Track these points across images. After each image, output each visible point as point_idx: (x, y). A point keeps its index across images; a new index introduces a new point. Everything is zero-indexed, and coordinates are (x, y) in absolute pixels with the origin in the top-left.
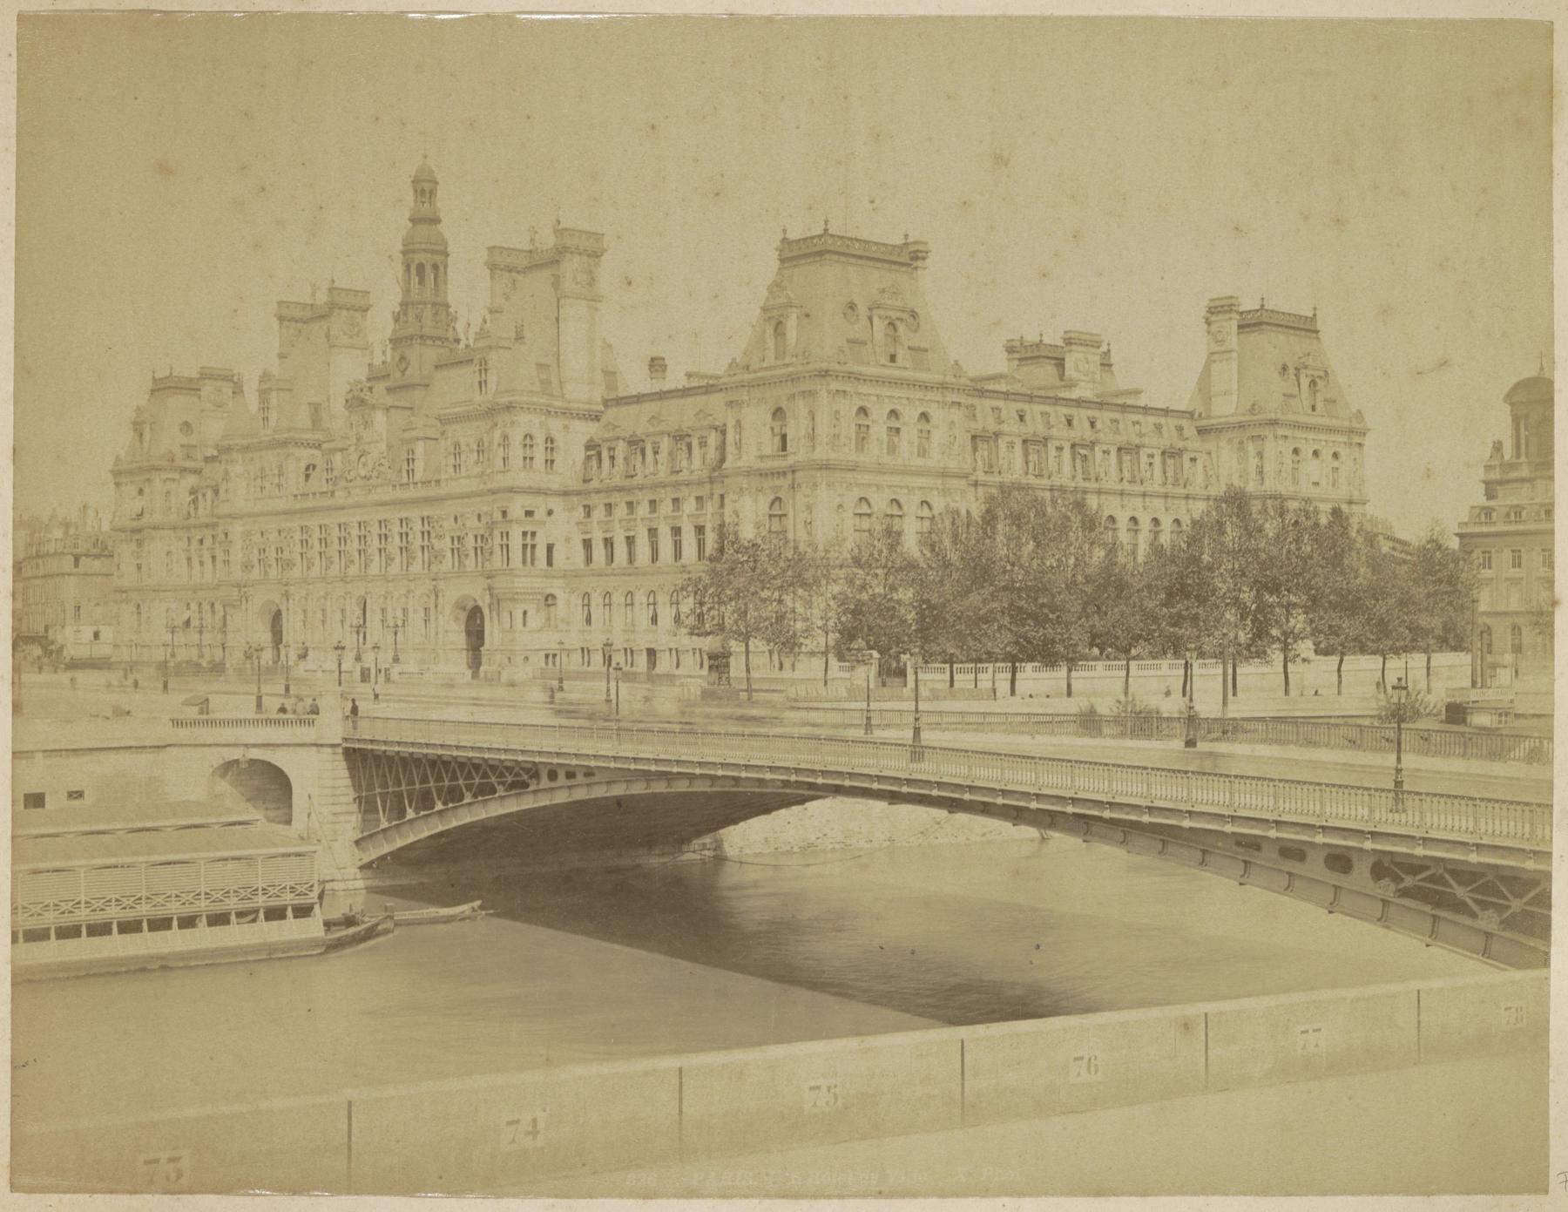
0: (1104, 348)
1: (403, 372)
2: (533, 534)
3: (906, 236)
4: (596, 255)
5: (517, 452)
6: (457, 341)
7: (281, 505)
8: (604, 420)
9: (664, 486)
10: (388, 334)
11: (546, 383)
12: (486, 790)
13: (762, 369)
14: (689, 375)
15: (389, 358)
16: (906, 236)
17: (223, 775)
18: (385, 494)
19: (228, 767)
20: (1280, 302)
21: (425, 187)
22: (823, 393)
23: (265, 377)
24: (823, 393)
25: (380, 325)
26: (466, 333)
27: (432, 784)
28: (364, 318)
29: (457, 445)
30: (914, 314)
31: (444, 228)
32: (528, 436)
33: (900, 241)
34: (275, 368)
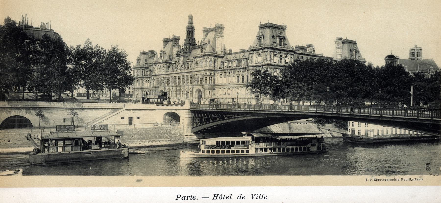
0: (313, 47)
1: (186, 50)
2: (211, 78)
3: (283, 24)
5: (208, 63)
6: (196, 45)
7: (164, 73)
8: (224, 58)
9: (236, 69)
10: (184, 43)
11: (214, 51)
12: (222, 118)
13: (256, 47)
14: (241, 50)
15: (184, 48)
16: (283, 24)
17: (167, 115)
18: (183, 71)
20: (350, 38)
21: (191, 18)
22: (269, 51)
23: (161, 51)
24: (269, 51)
25: (182, 42)
26: (198, 43)
27: (210, 117)
28: (179, 41)
29: (197, 62)
30: (284, 38)
31: (194, 25)
32: (211, 60)
34: (163, 49)
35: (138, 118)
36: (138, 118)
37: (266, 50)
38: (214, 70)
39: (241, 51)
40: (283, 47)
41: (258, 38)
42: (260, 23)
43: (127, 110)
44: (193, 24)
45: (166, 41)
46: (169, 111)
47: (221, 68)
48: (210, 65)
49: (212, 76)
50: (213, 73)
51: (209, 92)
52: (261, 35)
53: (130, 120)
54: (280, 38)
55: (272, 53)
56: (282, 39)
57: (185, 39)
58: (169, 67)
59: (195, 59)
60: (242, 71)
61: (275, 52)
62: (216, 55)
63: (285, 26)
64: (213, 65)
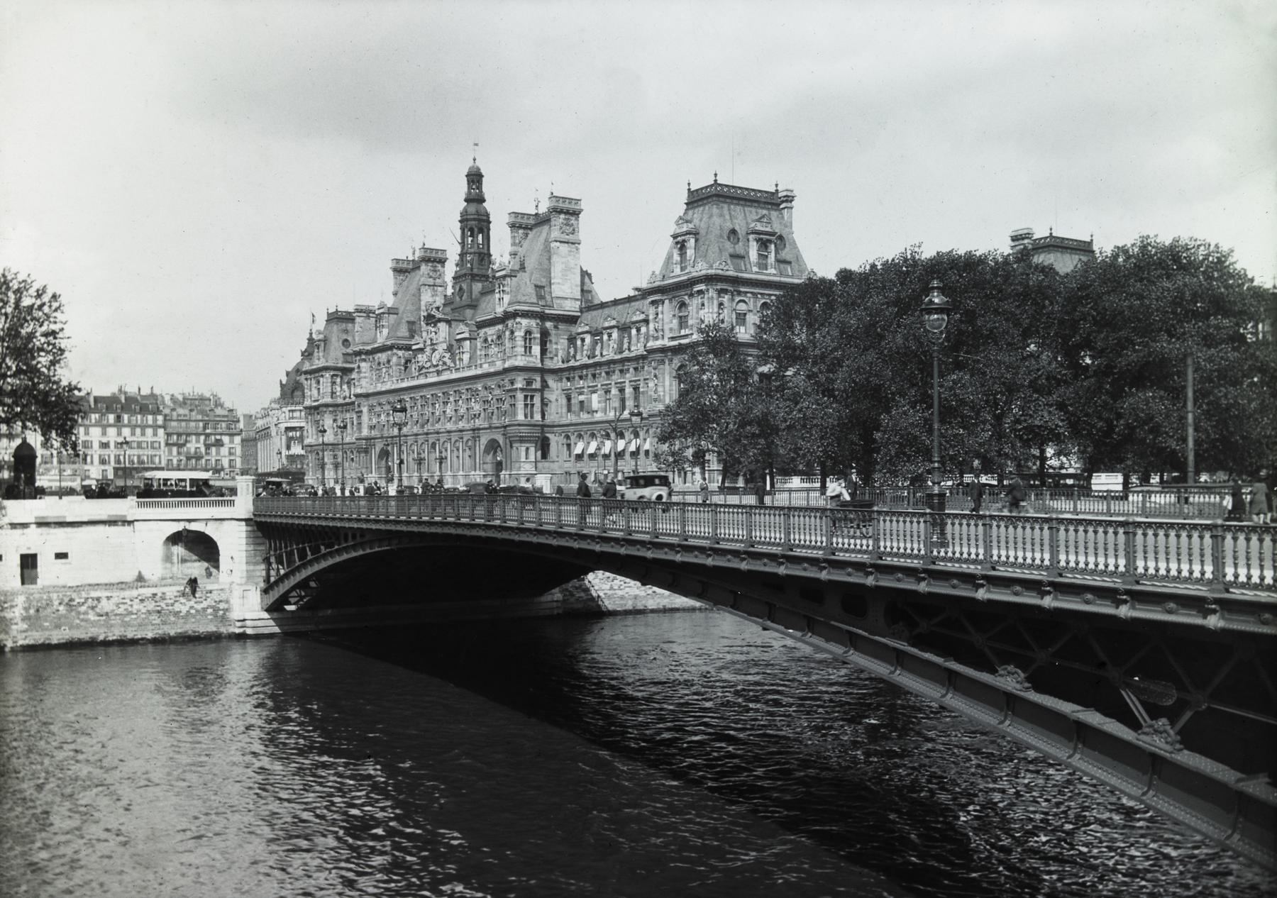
1: (461, 298)
2: (532, 397)
4: (576, 214)
11: (541, 297)
14: (637, 289)
19: (175, 539)
21: (475, 178)
25: (450, 270)
32: (528, 332)
33: (773, 190)
35: (61, 556)
36: (61, 556)
37: (702, 287)
38: (543, 371)
39: (632, 293)
40: (773, 271)
41: (677, 243)
42: (689, 184)
43: (14, 526)
44: (484, 201)
45: (402, 270)
46: (179, 527)
47: (568, 361)
48: (528, 349)
49: (536, 390)
50: (539, 379)
51: (524, 449)
52: (685, 228)
53: (29, 563)
54: (761, 239)
55: (726, 299)
56: (770, 241)
57: (458, 258)
58: (408, 361)
59: (482, 332)
60: (617, 372)
61: (739, 293)
62: (547, 311)
63: (789, 194)
64: (536, 349)
